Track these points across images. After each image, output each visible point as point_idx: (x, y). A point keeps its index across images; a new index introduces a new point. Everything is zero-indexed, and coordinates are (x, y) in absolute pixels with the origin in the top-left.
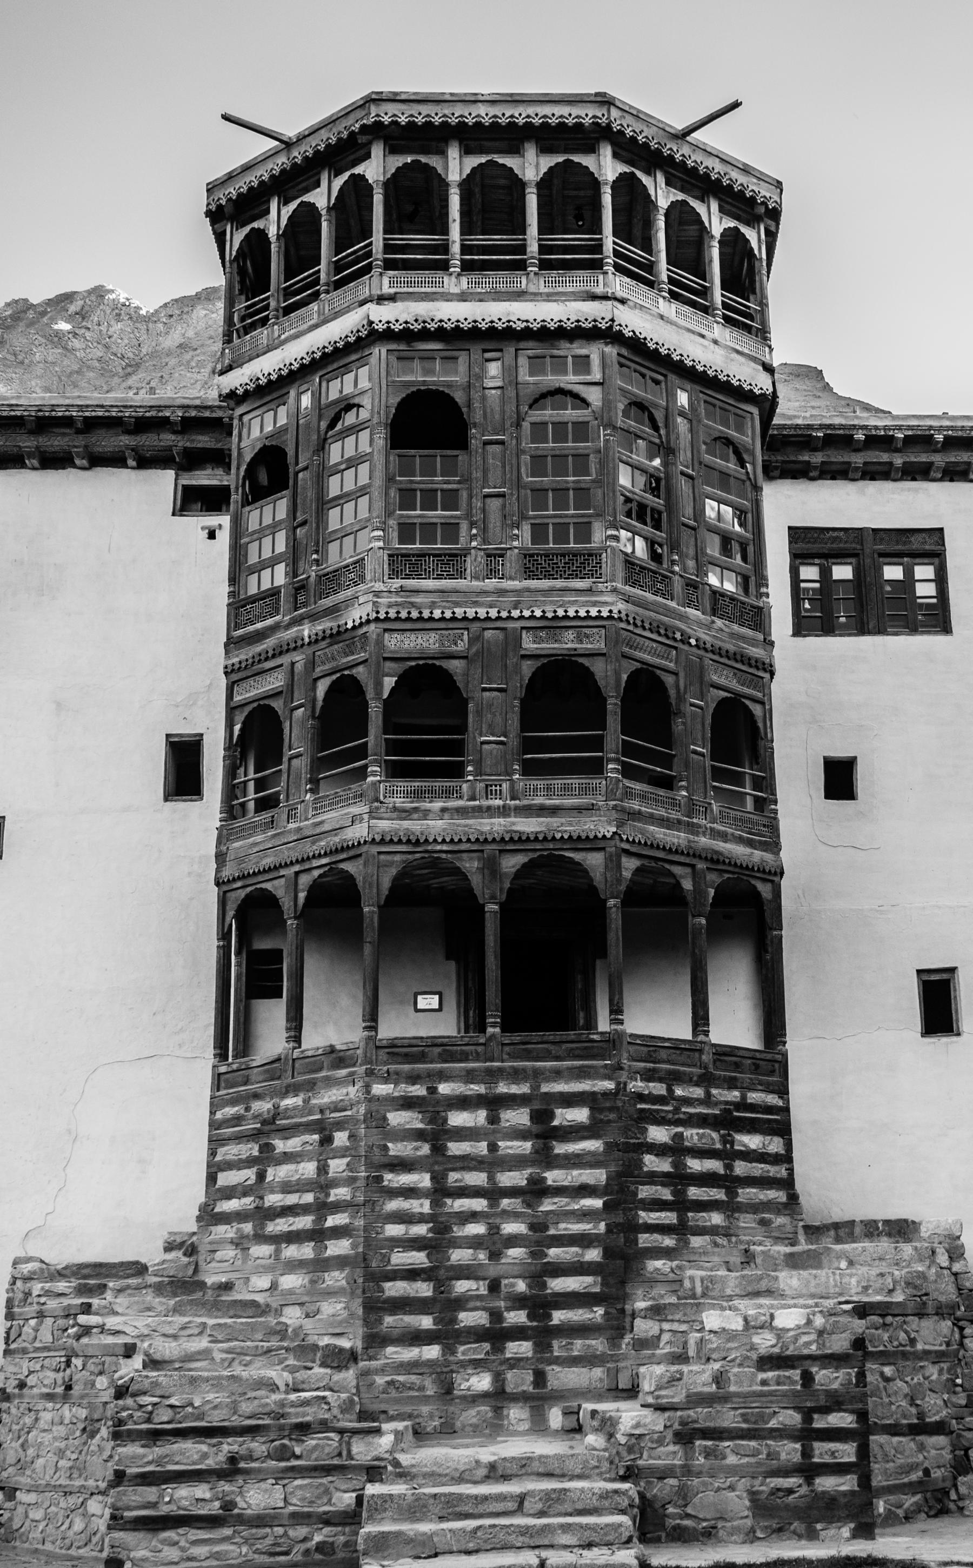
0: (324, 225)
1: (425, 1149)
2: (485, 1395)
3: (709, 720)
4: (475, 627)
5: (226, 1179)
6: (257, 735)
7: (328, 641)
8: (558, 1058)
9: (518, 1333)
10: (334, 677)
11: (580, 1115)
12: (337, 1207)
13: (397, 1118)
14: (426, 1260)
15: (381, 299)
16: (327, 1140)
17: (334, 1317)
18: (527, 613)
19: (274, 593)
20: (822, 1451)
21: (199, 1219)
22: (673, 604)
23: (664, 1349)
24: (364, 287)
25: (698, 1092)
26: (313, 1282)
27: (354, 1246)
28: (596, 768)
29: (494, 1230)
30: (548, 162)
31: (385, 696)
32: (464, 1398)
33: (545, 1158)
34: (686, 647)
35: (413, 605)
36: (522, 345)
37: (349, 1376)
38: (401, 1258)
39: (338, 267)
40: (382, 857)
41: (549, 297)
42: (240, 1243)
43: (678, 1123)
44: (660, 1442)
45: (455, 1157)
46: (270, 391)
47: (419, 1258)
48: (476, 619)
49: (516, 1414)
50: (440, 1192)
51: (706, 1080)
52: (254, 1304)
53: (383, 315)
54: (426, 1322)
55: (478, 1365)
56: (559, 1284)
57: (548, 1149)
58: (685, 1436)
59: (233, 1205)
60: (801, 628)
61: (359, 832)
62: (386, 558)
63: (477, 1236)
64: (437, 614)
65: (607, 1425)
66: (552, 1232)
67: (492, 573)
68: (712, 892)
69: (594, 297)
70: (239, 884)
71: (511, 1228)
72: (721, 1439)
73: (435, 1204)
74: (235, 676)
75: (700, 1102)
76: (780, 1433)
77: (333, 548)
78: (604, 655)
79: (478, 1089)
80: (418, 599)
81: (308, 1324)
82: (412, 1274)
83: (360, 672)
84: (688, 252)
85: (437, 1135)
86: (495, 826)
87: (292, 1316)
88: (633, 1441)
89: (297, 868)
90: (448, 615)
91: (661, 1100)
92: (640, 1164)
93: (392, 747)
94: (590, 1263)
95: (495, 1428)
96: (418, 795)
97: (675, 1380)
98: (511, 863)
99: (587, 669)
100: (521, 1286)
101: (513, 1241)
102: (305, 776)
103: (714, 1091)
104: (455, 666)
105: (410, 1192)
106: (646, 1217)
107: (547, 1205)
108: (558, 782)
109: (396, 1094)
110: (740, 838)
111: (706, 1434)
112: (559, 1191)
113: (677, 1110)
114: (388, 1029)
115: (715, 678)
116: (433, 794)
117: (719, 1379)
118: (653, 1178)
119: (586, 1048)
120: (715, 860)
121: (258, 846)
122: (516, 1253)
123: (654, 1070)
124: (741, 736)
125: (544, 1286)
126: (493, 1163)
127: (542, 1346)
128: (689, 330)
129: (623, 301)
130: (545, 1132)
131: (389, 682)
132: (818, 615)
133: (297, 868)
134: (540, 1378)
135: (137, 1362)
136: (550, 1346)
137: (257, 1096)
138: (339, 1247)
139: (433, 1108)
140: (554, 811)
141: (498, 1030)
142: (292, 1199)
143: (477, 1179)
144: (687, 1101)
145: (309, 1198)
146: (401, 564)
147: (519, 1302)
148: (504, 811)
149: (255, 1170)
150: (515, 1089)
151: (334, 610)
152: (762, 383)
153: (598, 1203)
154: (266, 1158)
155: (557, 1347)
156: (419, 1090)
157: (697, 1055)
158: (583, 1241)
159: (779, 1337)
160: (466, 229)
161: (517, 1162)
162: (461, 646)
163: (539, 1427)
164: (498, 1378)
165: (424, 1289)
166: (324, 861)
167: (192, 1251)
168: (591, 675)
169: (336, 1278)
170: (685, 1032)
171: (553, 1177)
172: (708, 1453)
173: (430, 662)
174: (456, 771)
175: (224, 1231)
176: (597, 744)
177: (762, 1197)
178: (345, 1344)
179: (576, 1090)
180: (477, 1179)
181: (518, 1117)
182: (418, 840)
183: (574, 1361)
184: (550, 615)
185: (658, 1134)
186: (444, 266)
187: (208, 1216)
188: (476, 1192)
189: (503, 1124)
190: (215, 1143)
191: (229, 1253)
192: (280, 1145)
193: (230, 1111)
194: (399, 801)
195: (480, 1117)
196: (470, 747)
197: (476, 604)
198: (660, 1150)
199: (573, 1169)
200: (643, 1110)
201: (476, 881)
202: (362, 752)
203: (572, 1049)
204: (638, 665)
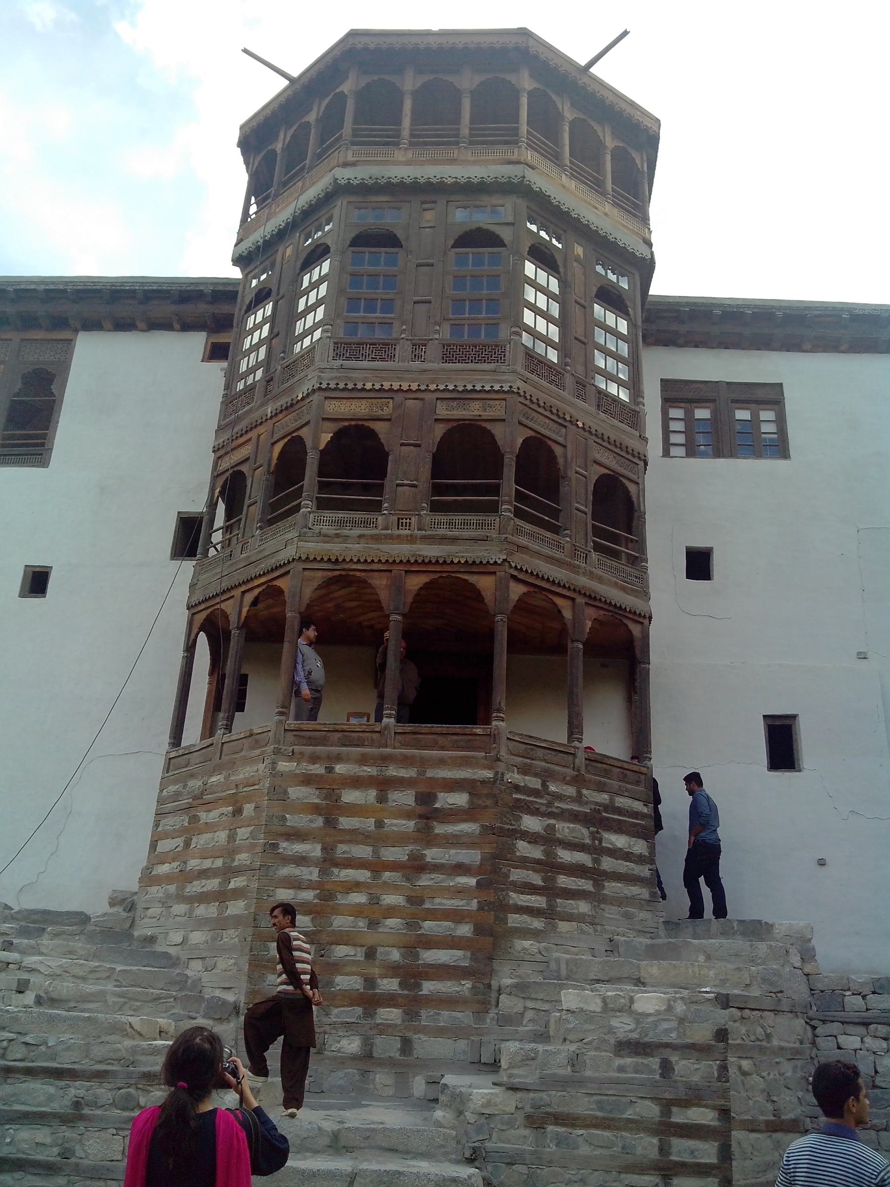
0: (313, 131)
1: (319, 822)
2: (354, 1058)
3: (591, 488)
4: (399, 397)
5: (165, 846)
7: (284, 413)
8: (443, 748)
9: (390, 1000)
10: (286, 440)
11: (460, 799)
13: (297, 792)
14: (311, 925)
15: (345, 165)
16: (238, 812)
18: (442, 387)
20: (682, 1149)
21: (141, 880)
22: (565, 394)
25: (571, 791)
26: (214, 939)
27: (247, 907)
28: (493, 508)
29: (375, 900)
31: (322, 447)
32: (335, 1058)
33: (426, 836)
34: (574, 427)
35: (350, 379)
36: (452, 198)
40: (306, 573)
41: (474, 163)
42: (166, 903)
43: (551, 815)
44: (511, 1124)
45: (344, 830)
48: (400, 390)
49: (382, 1078)
50: (329, 861)
51: (578, 781)
52: (166, 955)
56: (431, 956)
57: (429, 829)
58: (537, 1120)
59: (164, 869)
60: (666, 453)
61: (290, 552)
62: (332, 345)
63: (359, 904)
64: (369, 386)
65: (458, 1102)
66: (427, 905)
67: (416, 357)
68: (589, 624)
69: (510, 162)
70: (203, 607)
71: (391, 899)
72: (574, 1126)
74: (220, 452)
75: (573, 800)
76: (635, 1125)
78: (504, 420)
79: (369, 770)
80: (354, 375)
81: (206, 977)
85: (331, 811)
86: (402, 550)
87: (195, 969)
88: (483, 1120)
89: (243, 588)
90: (377, 387)
91: (535, 793)
92: (512, 849)
93: (323, 487)
94: (461, 938)
96: (341, 523)
97: (529, 1059)
98: (415, 582)
99: (489, 431)
100: (395, 955)
101: (391, 911)
102: (258, 517)
103: (585, 792)
104: (380, 428)
105: (301, 860)
107: (425, 880)
108: (459, 518)
109: (298, 772)
110: (616, 584)
111: (560, 1119)
112: (436, 868)
113: (550, 804)
115: (598, 456)
116: (354, 524)
117: (574, 1061)
118: (525, 863)
119: (469, 740)
120: (592, 599)
122: (391, 922)
123: (530, 765)
124: (618, 511)
125: (417, 956)
127: (411, 1014)
128: (585, 201)
129: (532, 168)
130: (427, 813)
131: (326, 438)
133: (243, 588)
136: (417, 1015)
137: (192, 776)
138: (237, 907)
139: (329, 787)
140: (454, 540)
141: (392, 720)
142: (207, 864)
143: (363, 851)
144: (559, 797)
145: (219, 863)
146: (346, 349)
147: (393, 970)
148: (411, 539)
149: (183, 838)
150: (403, 773)
153: (472, 881)
154: (194, 828)
155: (426, 1016)
156: (318, 769)
157: (570, 758)
158: (456, 916)
159: (638, 1022)
161: (401, 839)
162: (387, 411)
164: (367, 1043)
166: (263, 580)
167: (131, 907)
168: (492, 436)
169: (231, 936)
171: (432, 854)
172: (560, 1141)
173: (360, 423)
174: (376, 507)
175: (155, 891)
176: (495, 490)
177: (626, 892)
179: (458, 777)
180: (363, 851)
182: (337, 560)
183: (441, 1032)
184: (460, 389)
185: (531, 823)
187: (148, 878)
188: (361, 864)
189: (391, 804)
191: (156, 910)
192: (204, 817)
193: (172, 788)
194: (327, 529)
196: (387, 489)
197: (401, 379)
198: (533, 838)
199: (450, 848)
200: (518, 800)
201: (384, 596)
202: (298, 494)
203: (457, 741)
204: (532, 434)
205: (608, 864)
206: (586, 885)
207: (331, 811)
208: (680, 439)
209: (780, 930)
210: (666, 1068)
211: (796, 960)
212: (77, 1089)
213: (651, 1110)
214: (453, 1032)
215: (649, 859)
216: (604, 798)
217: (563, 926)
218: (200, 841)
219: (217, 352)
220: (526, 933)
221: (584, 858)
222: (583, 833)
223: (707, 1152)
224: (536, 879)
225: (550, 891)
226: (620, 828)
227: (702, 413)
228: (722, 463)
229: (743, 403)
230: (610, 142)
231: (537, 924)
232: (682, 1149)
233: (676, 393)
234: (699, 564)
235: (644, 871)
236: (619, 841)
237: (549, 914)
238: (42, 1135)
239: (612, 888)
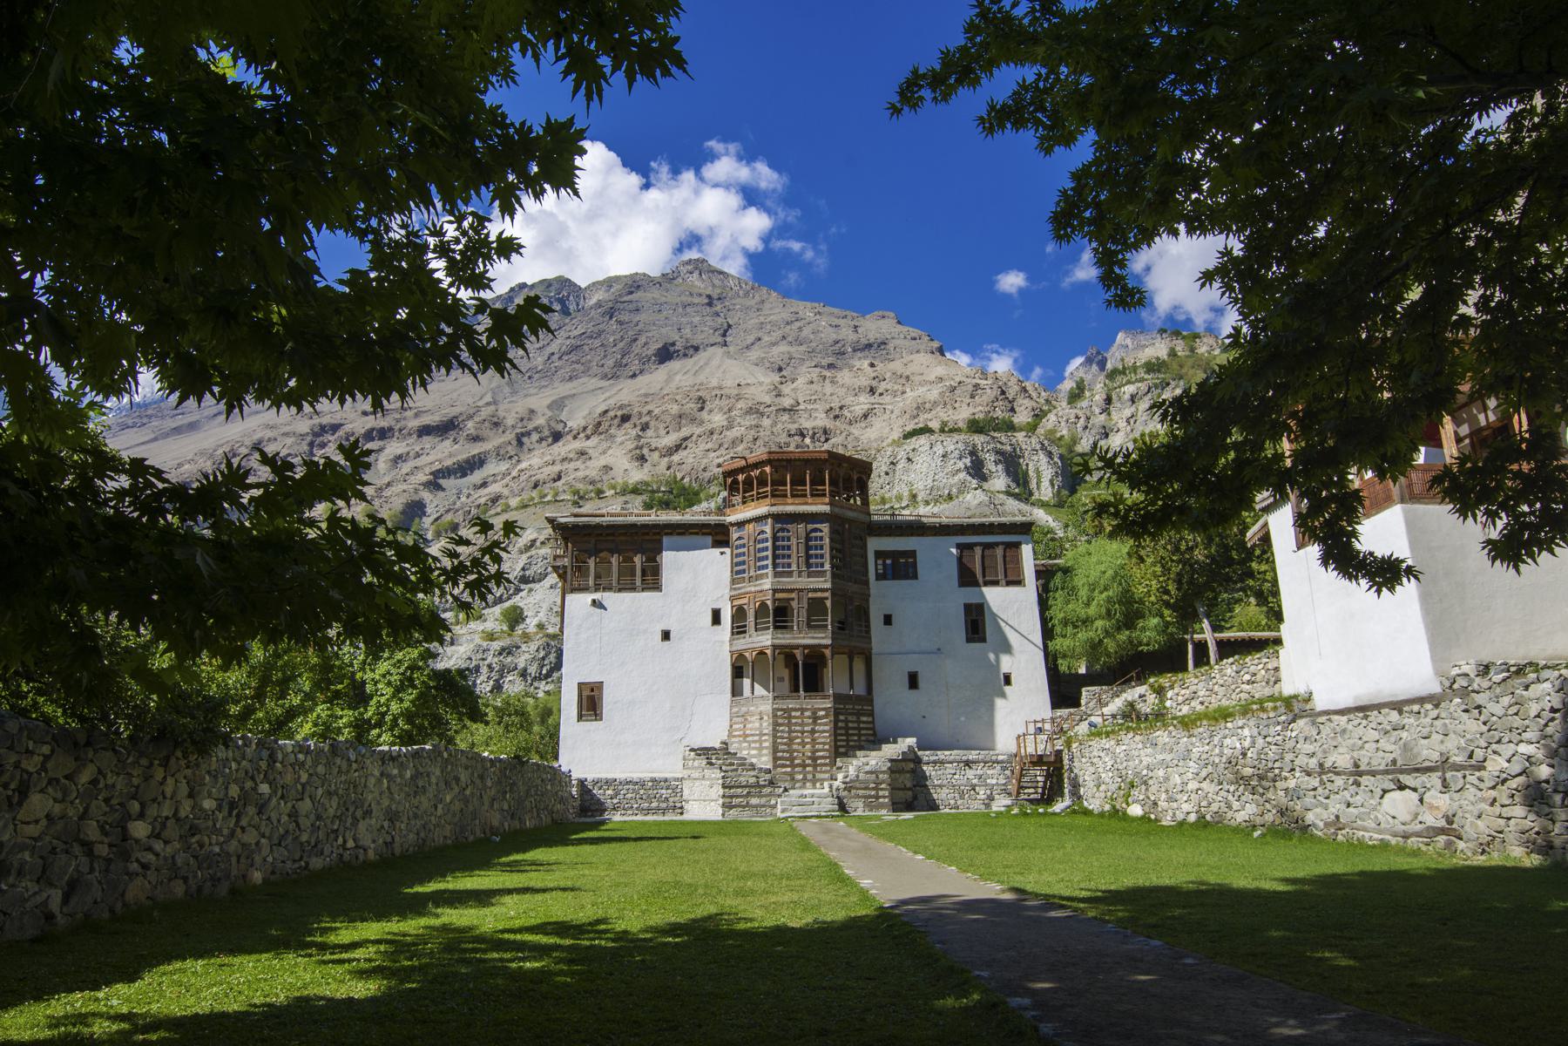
6: (739, 614)
17: (765, 761)
24: (768, 501)
33: (815, 722)
46: (741, 524)
50: (790, 732)
53: (775, 509)
74: (732, 599)
87: (754, 760)
95: (803, 787)
121: (742, 643)
130: (815, 718)
132: (879, 577)
181: (807, 714)
187: (730, 735)
225: (847, 734)
233: (878, 554)
234: (888, 620)
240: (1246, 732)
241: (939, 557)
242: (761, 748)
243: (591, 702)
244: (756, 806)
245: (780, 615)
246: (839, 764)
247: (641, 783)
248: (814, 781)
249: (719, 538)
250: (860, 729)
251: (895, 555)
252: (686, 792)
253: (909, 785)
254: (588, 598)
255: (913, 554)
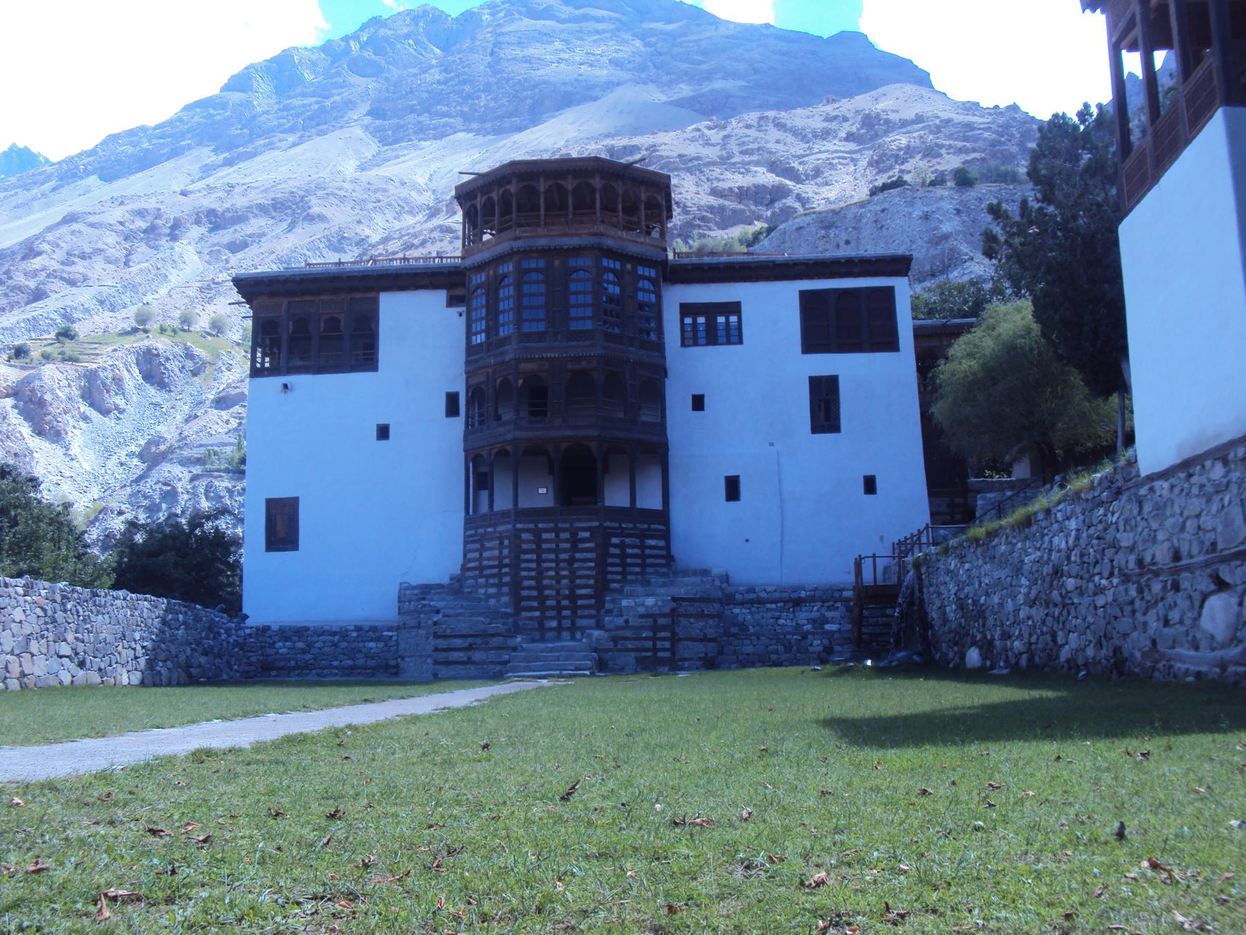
1: (534, 546)
5: (470, 556)
9: (566, 608)
11: (587, 534)
12: (506, 566)
13: (524, 536)
15: (517, 238)
16: (501, 543)
19: (481, 345)
23: (615, 613)
25: (631, 525)
30: (576, 182)
33: (574, 548)
37: (511, 620)
38: (526, 583)
39: (501, 223)
46: (479, 268)
47: (532, 583)
49: (565, 634)
50: (539, 561)
53: (518, 244)
54: (535, 604)
55: (553, 618)
56: (579, 592)
58: (615, 640)
60: (683, 345)
61: (510, 436)
65: (590, 636)
71: (563, 573)
73: (539, 565)
74: (469, 374)
77: (501, 329)
79: (551, 525)
82: (530, 588)
83: (510, 377)
84: (631, 209)
85: (538, 540)
95: (559, 638)
98: (564, 446)
100: (567, 592)
101: (564, 577)
106: (610, 569)
107: (576, 565)
114: (521, 505)
117: (627, 621)
118: (614, 556)
122: (565, 581)
126: (557, 551)
130: (574, 540)
131: (521, 381)
132: (690, 338)
134: (573, 623)
135: (440, 616)
142: (491, 563)
143: (552, 556)
147: (566, 597)
151: (501, 354)
152: (660, 257)
154: (482, 549)
155: (579, 612)
156: (531, 526)
158: (588, 577)
160: (546, 210)
161: (565, 551)
163: (573, 638)
164: (560, 624)
165: (534, 593)
169: (505, 589)
170: (628, 505)
171: (578, 555)
175: (471, 574)
178: (509, 610)
180: (552, 556)
185: (615, 540)
186: (539, 225)
187: (464, 568)
190: (466, 543)
192: (488, 545)
195: (553, 535)
198: (616, 546)
205: (647, 552)
206: (639, 561)
207: (538, 540)
208: (691, 334)
209: (715, 571)
210: (655, 621)
211: (718, 583)
212: (470, 640)
213: (650, 634)
214: (590, 617)
215: (668, 547)
216: (646, 526)
217: (629, 577)
218: (486, 554)
219: (452, 301)
220: (614, 581)
221: (637, 551)
222: (637, 541)
223: (667, 644)
224: (618, 561)
225: (624, 565)
226: (651, 537)
227: (701, 320)
228: (709, 348)
229: (721, 314)
230: (643, 196)
231: (619, 577)
232: (659, 644)
233: (687, 309)
235: (664, 552)
236: (652, 542)
237: (624, 573)
238: (461, 654)
239: (649, 561)
240: (1073, 524)
241: (772, 311)
242: (500, 585)
243: (283, 525)
244: (483, 663)
245: (536, 397)
246: (608, 606)
247: (343, 633)
248: (573, 629)
249: (458, 292)
250: (643, 557)
251: (712, 310)
252: (402, 645)
253: (711, 632)
254: (277, 381)
255: (734, 308)
